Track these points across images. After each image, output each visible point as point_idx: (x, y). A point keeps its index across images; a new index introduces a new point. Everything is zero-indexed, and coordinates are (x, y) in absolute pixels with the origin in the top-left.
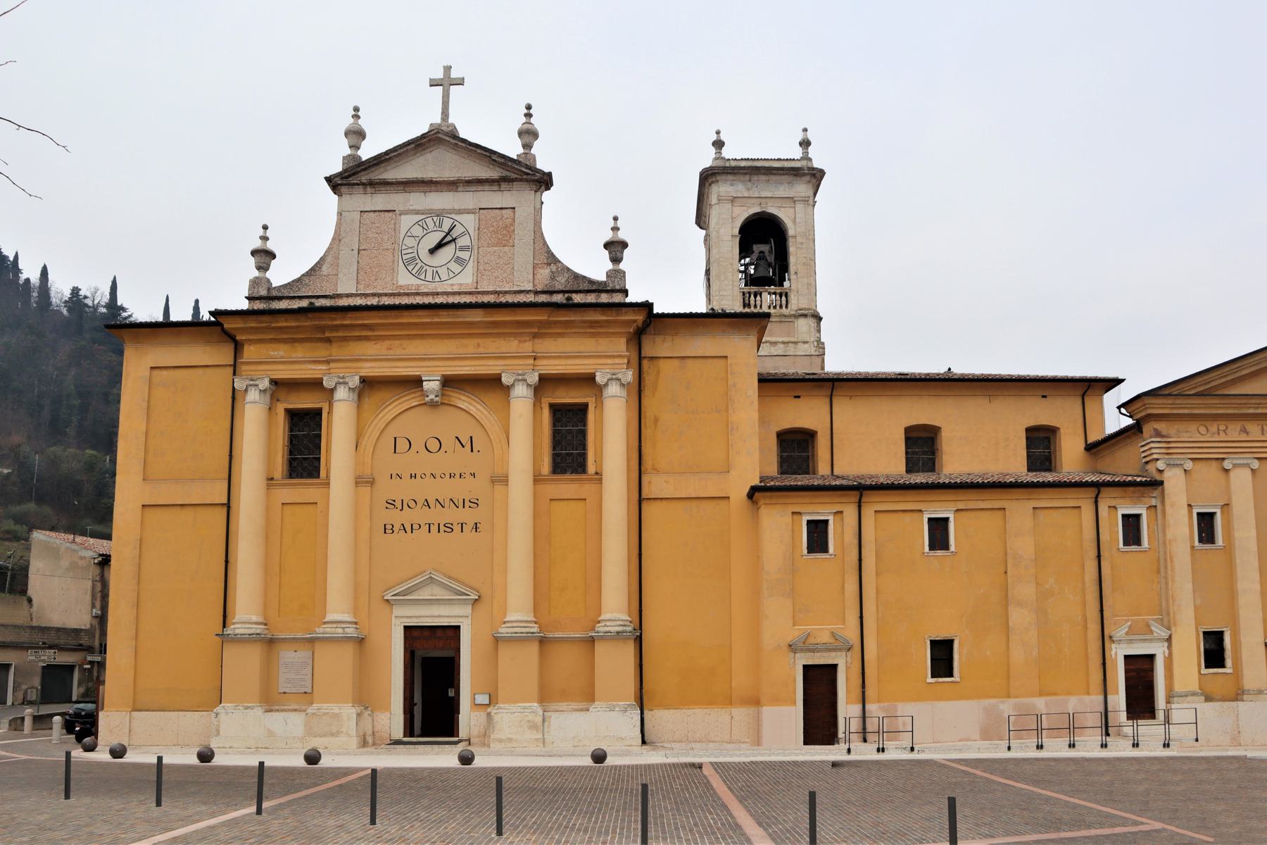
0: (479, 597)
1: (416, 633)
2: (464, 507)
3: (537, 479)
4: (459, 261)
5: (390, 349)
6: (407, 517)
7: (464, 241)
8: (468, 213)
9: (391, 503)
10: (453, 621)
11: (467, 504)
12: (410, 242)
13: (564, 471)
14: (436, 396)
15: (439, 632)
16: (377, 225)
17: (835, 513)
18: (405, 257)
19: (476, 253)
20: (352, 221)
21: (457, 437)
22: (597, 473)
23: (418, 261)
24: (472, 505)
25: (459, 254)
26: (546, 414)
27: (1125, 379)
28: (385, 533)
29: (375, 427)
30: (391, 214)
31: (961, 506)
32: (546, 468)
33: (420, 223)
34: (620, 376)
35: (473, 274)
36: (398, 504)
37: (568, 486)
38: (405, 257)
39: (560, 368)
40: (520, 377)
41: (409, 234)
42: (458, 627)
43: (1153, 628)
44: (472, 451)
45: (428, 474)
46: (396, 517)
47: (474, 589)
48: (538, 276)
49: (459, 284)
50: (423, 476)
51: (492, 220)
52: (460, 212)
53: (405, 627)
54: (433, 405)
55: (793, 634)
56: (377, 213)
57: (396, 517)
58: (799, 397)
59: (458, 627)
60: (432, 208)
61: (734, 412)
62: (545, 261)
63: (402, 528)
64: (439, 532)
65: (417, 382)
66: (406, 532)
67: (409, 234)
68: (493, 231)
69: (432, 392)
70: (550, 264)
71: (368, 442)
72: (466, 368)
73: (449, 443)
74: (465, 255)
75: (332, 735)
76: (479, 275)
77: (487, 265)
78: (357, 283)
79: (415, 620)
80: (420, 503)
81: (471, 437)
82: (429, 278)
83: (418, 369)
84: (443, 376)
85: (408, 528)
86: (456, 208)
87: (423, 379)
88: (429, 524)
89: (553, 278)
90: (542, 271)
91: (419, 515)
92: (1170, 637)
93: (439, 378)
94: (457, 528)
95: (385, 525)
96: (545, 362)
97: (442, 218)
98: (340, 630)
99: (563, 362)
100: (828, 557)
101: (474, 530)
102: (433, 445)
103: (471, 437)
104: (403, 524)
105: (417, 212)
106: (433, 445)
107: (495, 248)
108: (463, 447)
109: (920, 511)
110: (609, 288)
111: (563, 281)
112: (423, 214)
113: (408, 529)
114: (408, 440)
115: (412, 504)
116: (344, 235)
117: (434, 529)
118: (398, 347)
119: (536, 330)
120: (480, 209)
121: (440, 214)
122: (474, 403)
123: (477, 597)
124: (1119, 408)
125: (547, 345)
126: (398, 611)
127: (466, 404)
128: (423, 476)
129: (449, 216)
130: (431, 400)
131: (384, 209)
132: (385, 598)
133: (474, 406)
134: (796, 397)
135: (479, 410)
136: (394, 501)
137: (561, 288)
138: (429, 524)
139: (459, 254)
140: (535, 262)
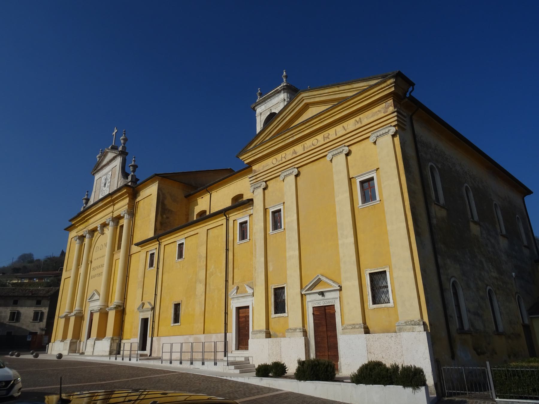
31: (186, 236)
92: (253, 293)
93: (100, 226)
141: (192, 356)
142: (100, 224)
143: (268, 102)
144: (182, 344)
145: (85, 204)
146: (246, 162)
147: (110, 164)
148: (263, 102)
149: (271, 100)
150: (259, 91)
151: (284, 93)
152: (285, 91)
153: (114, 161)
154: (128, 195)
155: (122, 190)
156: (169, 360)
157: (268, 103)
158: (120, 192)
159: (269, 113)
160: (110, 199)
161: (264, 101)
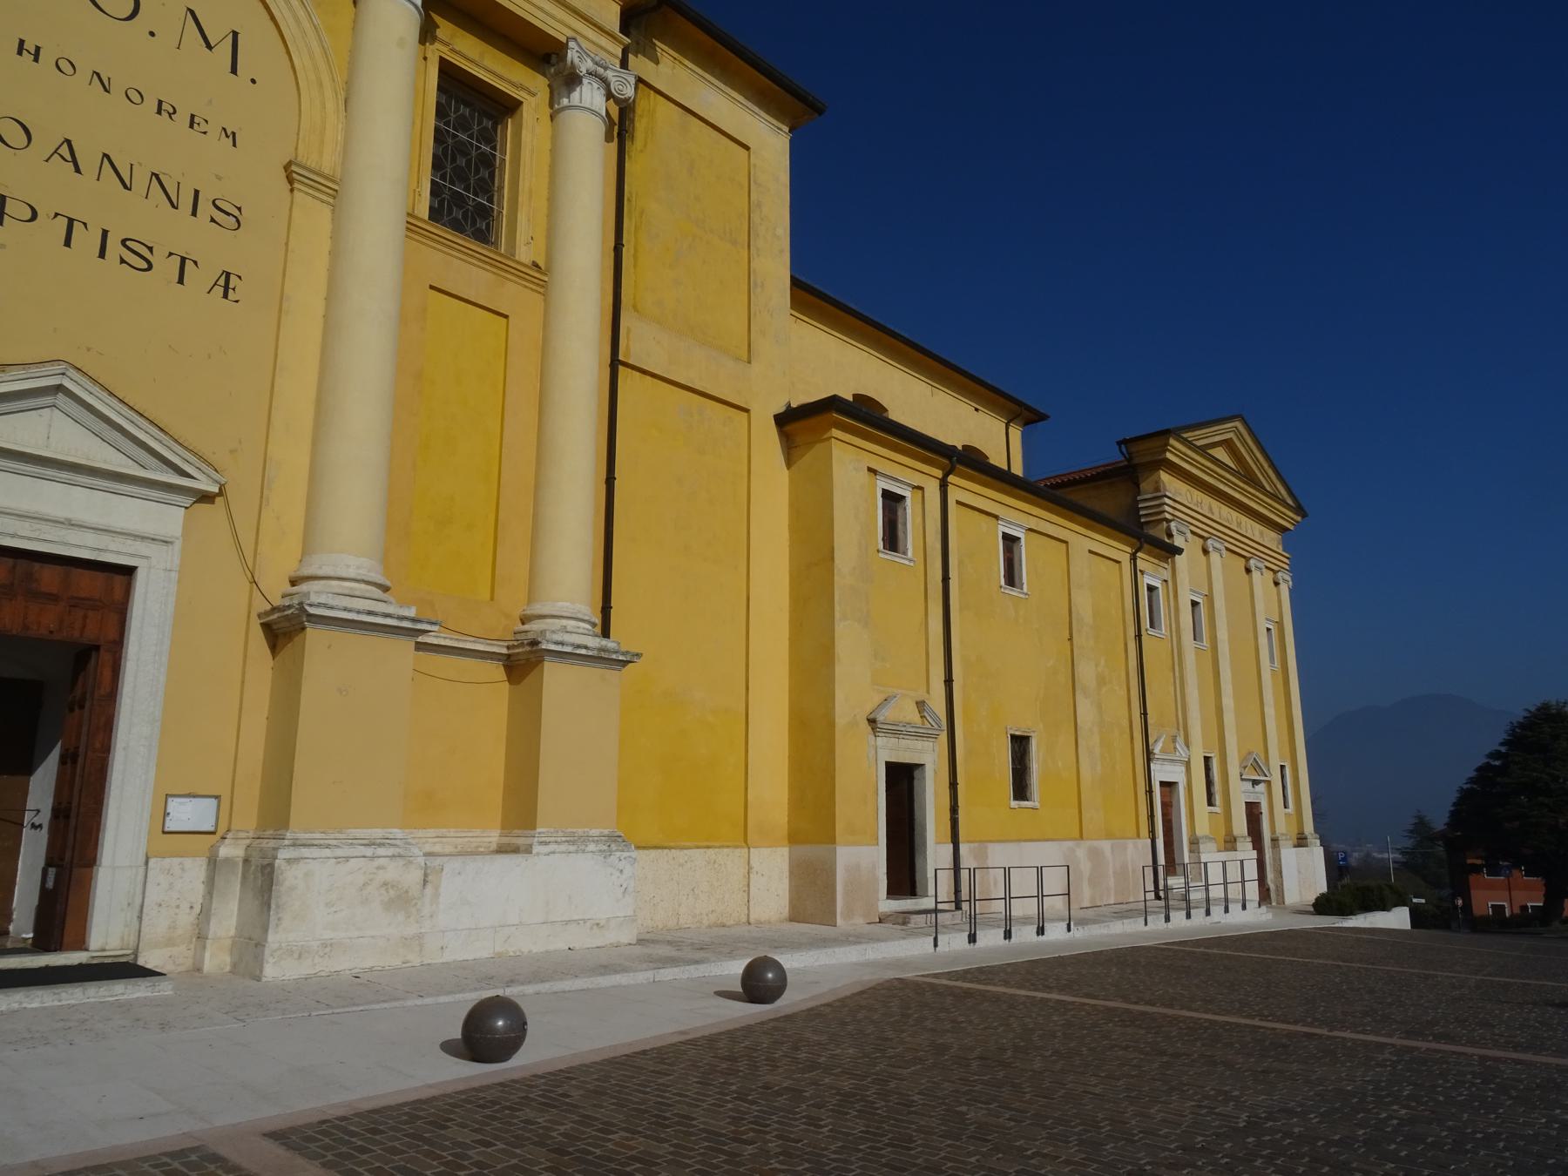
10: (112, 547)
15: (49, 578)
24: (219, 216)
27: (1048, 417)
32: (423, 210)
34: (609, 74)
42: (129, 572)
43: (1178, 747)
59: (129, 572)
61: (758, 256)
64: (102, 254)
80: (45, 143)
94: (166, 268)
100: (907, 562)
101: (219, 291)
109: (997, 517)
117: (86, 240)
124: (1119, 443)
141: (1041, 905)
144: (1040, 870)
146: (1169, 455)
156: (1063, 920)
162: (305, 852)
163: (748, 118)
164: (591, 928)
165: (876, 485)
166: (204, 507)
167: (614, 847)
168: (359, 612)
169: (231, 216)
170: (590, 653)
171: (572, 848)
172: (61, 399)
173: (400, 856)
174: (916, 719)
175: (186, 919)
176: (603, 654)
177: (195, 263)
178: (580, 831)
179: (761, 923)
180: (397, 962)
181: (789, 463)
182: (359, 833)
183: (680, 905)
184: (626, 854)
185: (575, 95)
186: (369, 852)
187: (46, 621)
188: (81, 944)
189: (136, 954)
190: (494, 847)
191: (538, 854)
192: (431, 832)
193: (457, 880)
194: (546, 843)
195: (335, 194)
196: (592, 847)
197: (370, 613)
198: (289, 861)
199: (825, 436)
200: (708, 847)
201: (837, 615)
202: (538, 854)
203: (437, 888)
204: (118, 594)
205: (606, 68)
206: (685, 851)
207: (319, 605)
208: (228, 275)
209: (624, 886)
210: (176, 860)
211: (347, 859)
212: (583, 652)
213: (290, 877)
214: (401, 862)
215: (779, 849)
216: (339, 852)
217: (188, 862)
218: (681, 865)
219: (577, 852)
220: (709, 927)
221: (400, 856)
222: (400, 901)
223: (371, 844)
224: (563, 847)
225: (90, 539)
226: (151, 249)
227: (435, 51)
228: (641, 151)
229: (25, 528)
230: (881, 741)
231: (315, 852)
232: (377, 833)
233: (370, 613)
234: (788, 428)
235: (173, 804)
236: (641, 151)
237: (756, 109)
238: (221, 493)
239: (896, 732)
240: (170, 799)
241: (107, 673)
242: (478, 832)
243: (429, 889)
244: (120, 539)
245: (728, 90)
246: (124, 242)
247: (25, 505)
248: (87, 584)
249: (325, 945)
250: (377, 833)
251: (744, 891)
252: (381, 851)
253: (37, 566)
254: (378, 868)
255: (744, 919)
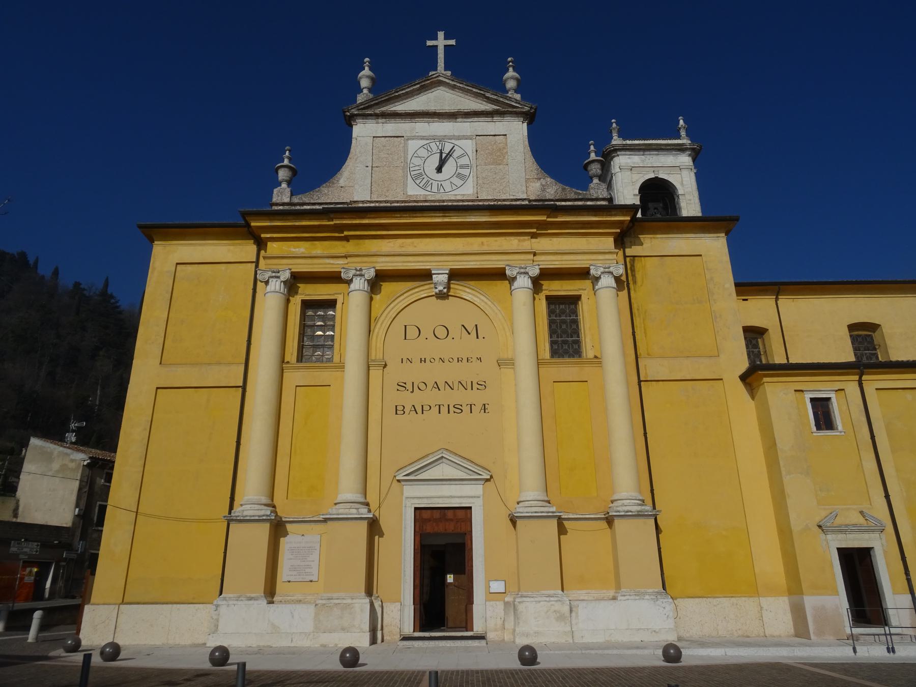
0: (491, 477)
1: (426, 515)
2: (472, 389)
3: (539, 363)
4: (460, 176)
5: (403, 247)
6: (418, 398)
7: (464, 161)
8: (466, 139)
9: (402, 386)
10: (464, 502)
11: (475, 386)
12: (417, 161)
13: (561, 356)
14: (444, 288)
15: (450, 514)
16: (388, 148)
17: (836, 391)
18: (413, 173)
19: (475, 170)
20: (366, 144)
21: (463, 326)
22: (596, 357)
23: (425, 176)
24: (479, 387)
25: (460, 171)
26: (542, 305)
28: (396, 414)
29: (386, 317)
30: (399, 139)
32: (546, 353)
33: (425, 147)
34: (611, 269)
35: (474, 187)
36: (409, 386)
37: (567, 369)
38: (413, 173)
39: (557, 263)
40: (522, 270)
41: (415, 155)
44: (478, 338)
45: (437, 359)
46: (407, 399)
47: (487, 470)
48: (531, 188)
49: (461, 195)
50: (432, 360)
51: (488, 144)
52: (459, 138)
53: (416, 509)
54: (441, 296)
55: (819, 515)
56: (387, 139)
57: (407, 399)
58: (746, 300)
59: (470, 508)
60: (435, 134)
61: (715, 303)
62: (536, 177)
63: (413, 409)
64: (449, 413)
65: (425, 276)
66: (417, 413)
67: (415, 155)
68: (489, 153)
69: (440, 284)
70: (540, 179)
71: (379, 330)
72: (472, 263)
73: (455, 331)
74: (465, 172)
75: (343, 629)
76: (479, 188)
77: (485, 180)
78: (371, 193)
79: (425, 501)
80: (430, 386)
81: (476, 325)
82: (435, 189)
83: (428, 264)
84: (451, 270)
85: (419, 410)
86: (456, 134)
87: (433, 272)
88: (439, 405)
89: (543, 190)
90: (533, 184)
91: (429, 397)
93: (447, 272)
94: (466, 409)
95: (396, 406)
96: (543, 258)
97: (443, 143)
98: (354, 511)
99: (559, 257)
100: (838, 434)
102: (441, 332)
103: (476, 325)
104: (414, 406)
105: (423, 138)
106: (441, 332)
107: (493, 166)
108: (469, 334)
110: (593, 197)
111: (552, 192)
112: (427, 140)
113: (419, 411)
114: (417, 327)
115: (422, 386)
116: (359, 155)
117: (444, 410)
118: (410, 245)
119: (534, 230)
120: (476, 136)
121: (442, 139)
122: (478, 295)
123: (489, 477)
125: (543, 243)
126: (410, 491)
127: (470, 296)
128: (432, 360)
129: (449, 141)
130: (440, 291)
131: (394, 135)
132: (397, 478)
133: (477, 297)
134: (744, 300)
135: (483, 301)
136: (405, 383)
137: (551, 198)
138: (439, 405)
139: (460, 171)
140: (527, 177)
142: (451, 269)
143: (650, 154)
145: (286, 181)
147: (458, 120)
148: (639, 150)
149: (658, 154)
150: (614, 125)
151: (689, 155)
152: (693, 154)
153: (490, 119)
154: (619, 231)
155: (613, 213)
157: (648, 156)
158: (595, 216)
159: (652, 176)
160: (544, 218)
161: (644, 150)
162: (524, 599)
163: (698, 242)
164: (652, 633)
165: (805, 397)
166: (488, 483)
167: (659, 597)
168: (532, 513)
169: (483, 385)
170: (634, 514)
171: (637, 598)
172: (444, 460)
173: (559, 601)
174: (861, 520)
175: (500, 622)
176: (640, 513)
177: (474, 405)
178: (643, 590)
179: (774, 637)
180: (564, 641)
181: (753, 398)
182: (543, 592)
183: (718, 625)
184: (664, 600)
185: (600, 283)
186: (547, 599)
187: (451, 527)
188: (472, 630)
189: (486, 633)
190: (611, 597)
191: (620, 600)
192: (584, 591)
193: (583, 611)
194: (624, 596)
195: (513, 364)
196: (647, 597)
197: (536, 512)
198: (519, 602)
199: (762, 382)
200: (732, 597)
201: (784, 473)
202: (620, 600)
203: (577, 613)
204: (469, 515)
205: (609, 268)
206: (717, 599)
207: (518, 512)
208: (485, 405)
209: (667, 615)
210: (494, 602)
211: (540, 602)
212: (630, 514)
213: (521, 608)
214: (560, 603)
215: (781, 598)
216: (536, 599)
217: (498, 603)
218: (715, 606)
219: (640, 599)
220: (739, 637)
221: (559, 601)
222: (561, 618)
223: (549, 596)
224: (632, 597)
225: (458, 500)
226: (461, 405)
227: (542, 297)
228: (641, 286)
229: (440, 500)
230: (829, 537)
231: (528, 599)
232: (552, 592)
233: (536, 512)
234: (748, 381)
235: (492, 584)
236: (641, 286)
237: (702, 235)
238: (491, 477)
239: (842, 530)
240: (504, 582)
241: (469, 541)
242: (605, 591)
243: (573, 614)
244: (465, 498)
245: (684, 235)
246: (454, 407)
247: (440, 494)
248: (460, 514)
249: (535, 633)
250: (552, 592)
251: (760, 619)
252: (552, 599)
253: (446, 511)
254: (552, 605)
255: (762, 634)
